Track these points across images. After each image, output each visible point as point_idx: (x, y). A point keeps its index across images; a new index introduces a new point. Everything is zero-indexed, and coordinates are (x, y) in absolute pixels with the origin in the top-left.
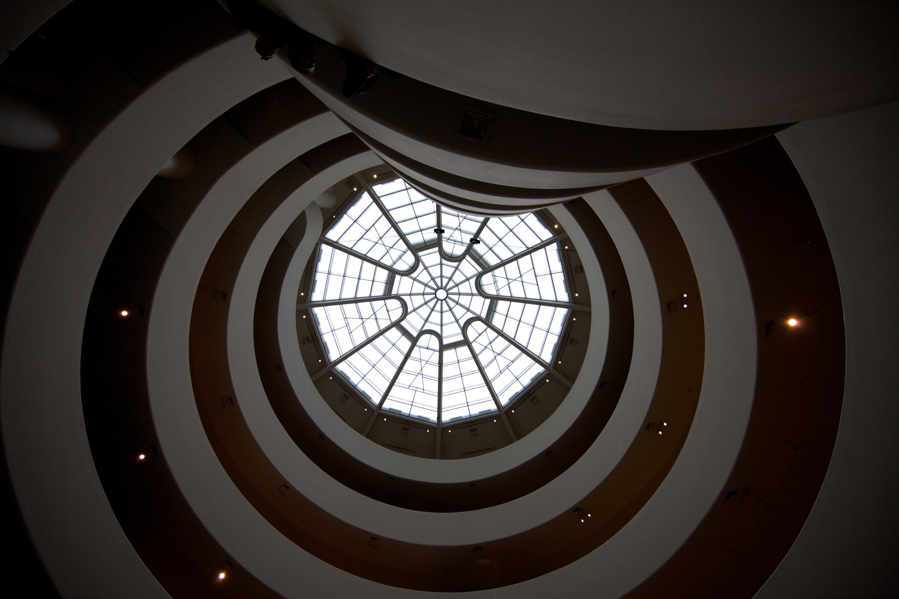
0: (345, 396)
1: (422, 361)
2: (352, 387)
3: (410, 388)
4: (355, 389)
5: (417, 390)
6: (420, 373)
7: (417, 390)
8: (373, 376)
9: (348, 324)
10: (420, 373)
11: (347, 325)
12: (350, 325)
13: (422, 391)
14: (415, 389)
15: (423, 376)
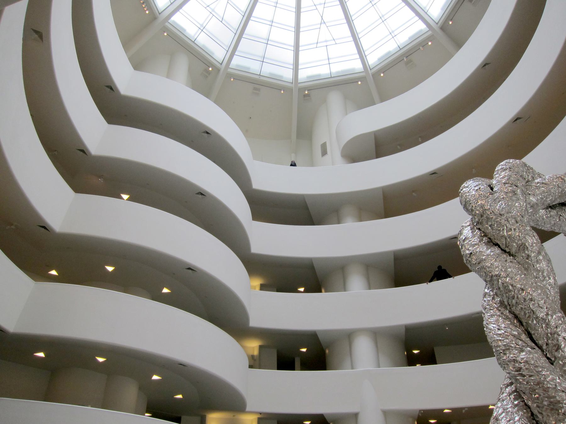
0: (255, 89)
1: (318, 7)
2: (257, 77)
3: (319, 45)
4: (262, 78)
5: (328, 43)
6: (323, 22)
7: (328, 43)
8: (273, 52)
9: (213, 10)
10: (323, 22)
11: (212, 13)
12: (216, 10)
13: (333, 42)
14: (325, 44)
15: (328, 24)
